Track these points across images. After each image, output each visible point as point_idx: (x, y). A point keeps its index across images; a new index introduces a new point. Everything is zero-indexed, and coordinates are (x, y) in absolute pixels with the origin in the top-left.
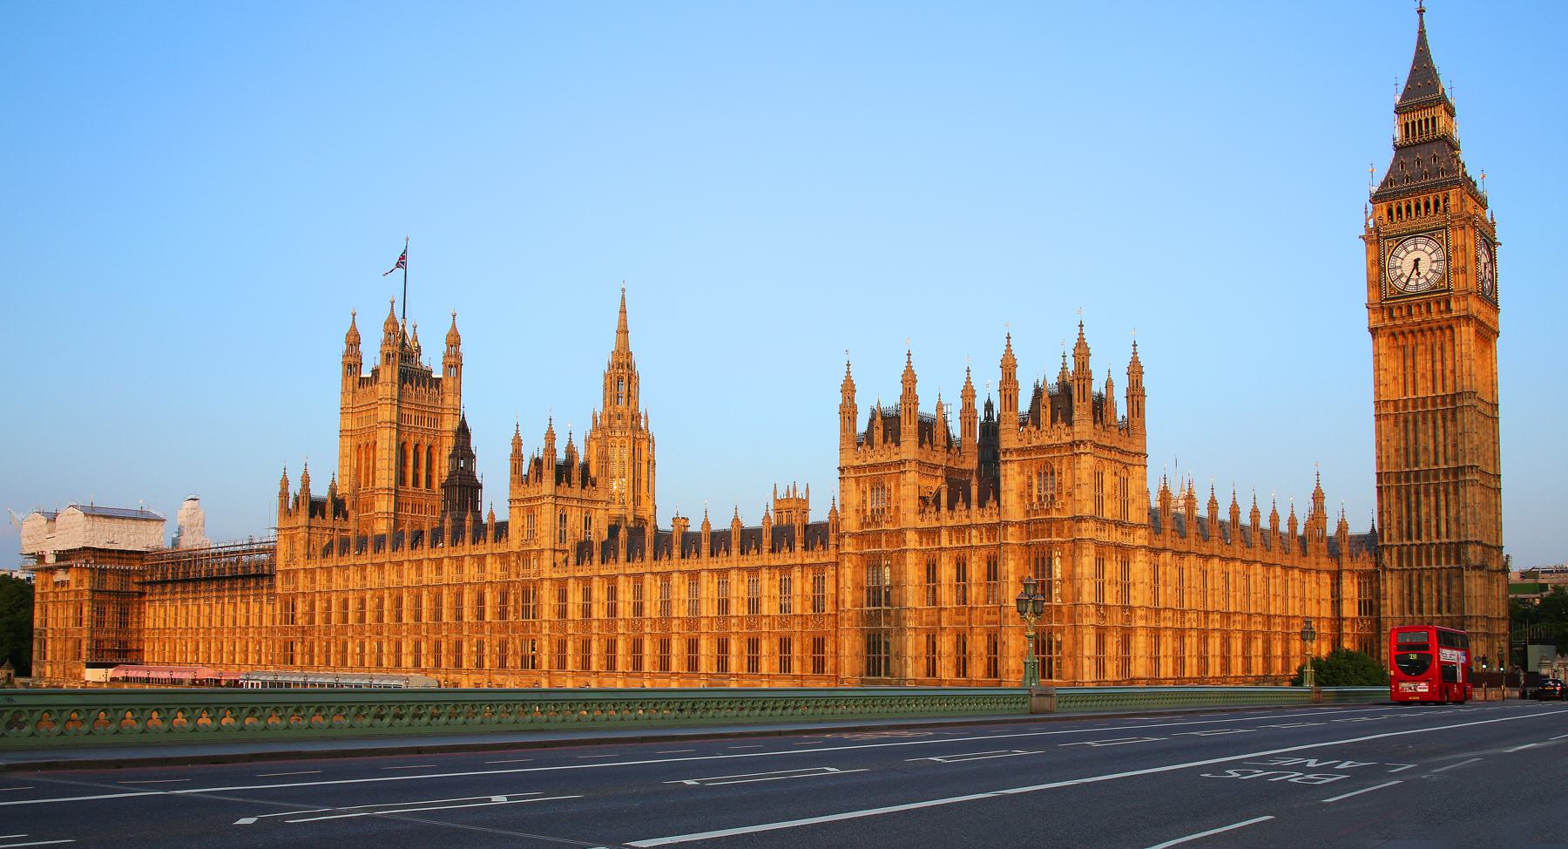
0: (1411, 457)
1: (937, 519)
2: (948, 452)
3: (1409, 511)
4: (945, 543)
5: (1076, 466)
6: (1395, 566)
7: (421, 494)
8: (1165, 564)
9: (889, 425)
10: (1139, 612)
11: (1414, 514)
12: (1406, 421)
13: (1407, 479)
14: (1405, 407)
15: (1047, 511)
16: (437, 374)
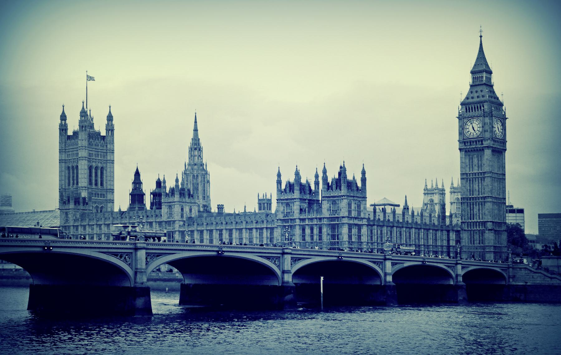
0: (471, 192)
1: (305, 216)
2: (310, 194)
3: (470, 210)
4: (307, 222)
5: (342, 202)
6: (467, 229)
7: (98, 189)
8: (374, 229)
9: (290, 187)
10: (364, 243)
11: (472, 211)
12: (470, 181)
13: (470, 200)
14: (470, 176)
15: (335, 215)
16: (103, 133)
